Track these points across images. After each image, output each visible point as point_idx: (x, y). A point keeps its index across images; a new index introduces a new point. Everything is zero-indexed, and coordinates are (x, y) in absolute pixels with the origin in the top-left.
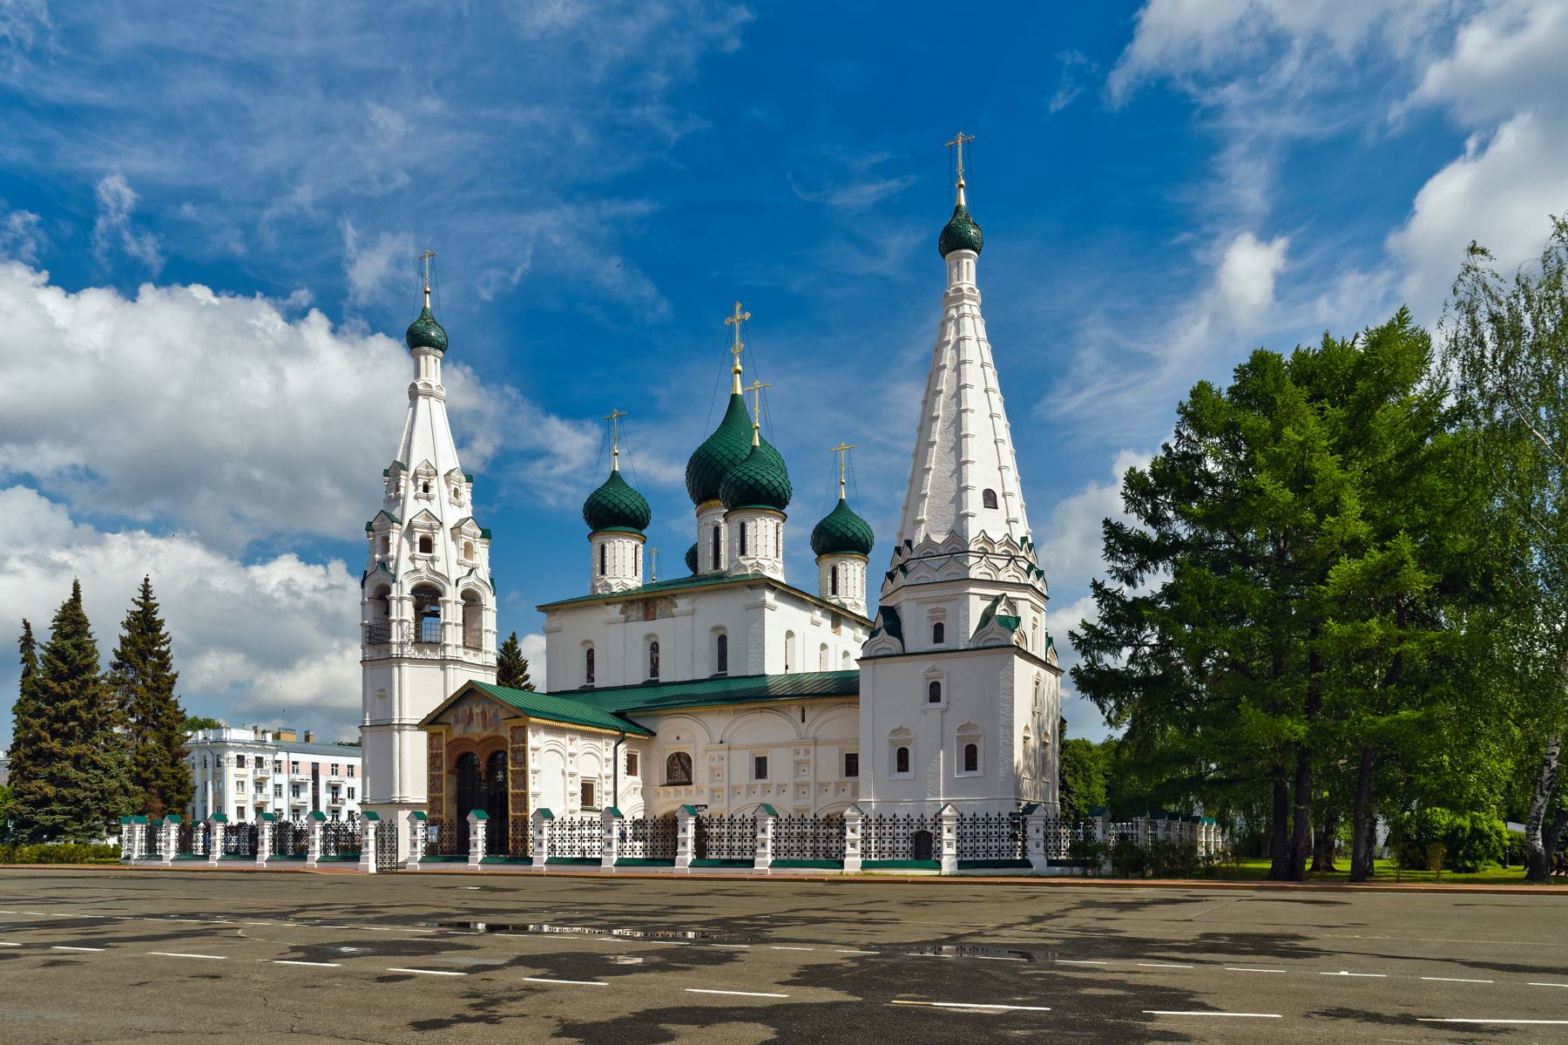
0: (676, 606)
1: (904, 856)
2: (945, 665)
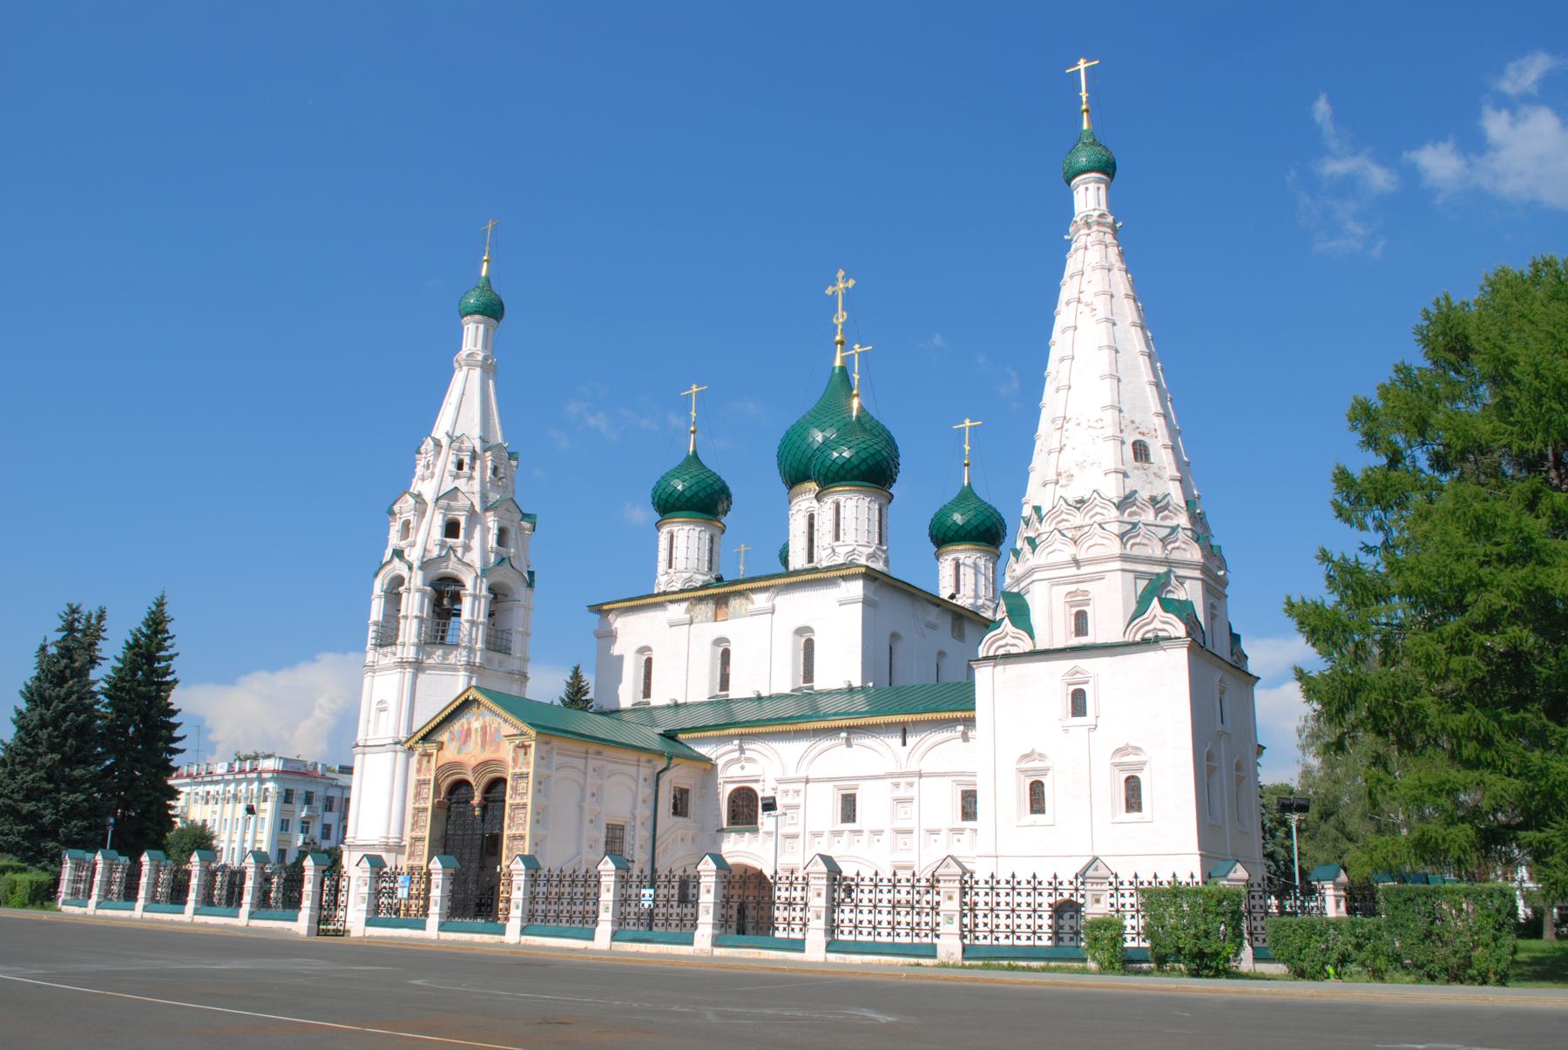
0: (753, 603)
2: (1091, 666)
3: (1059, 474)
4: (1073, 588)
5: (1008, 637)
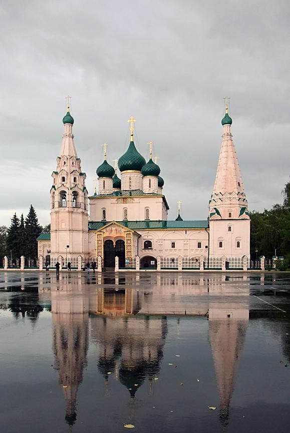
5: (216, 216)
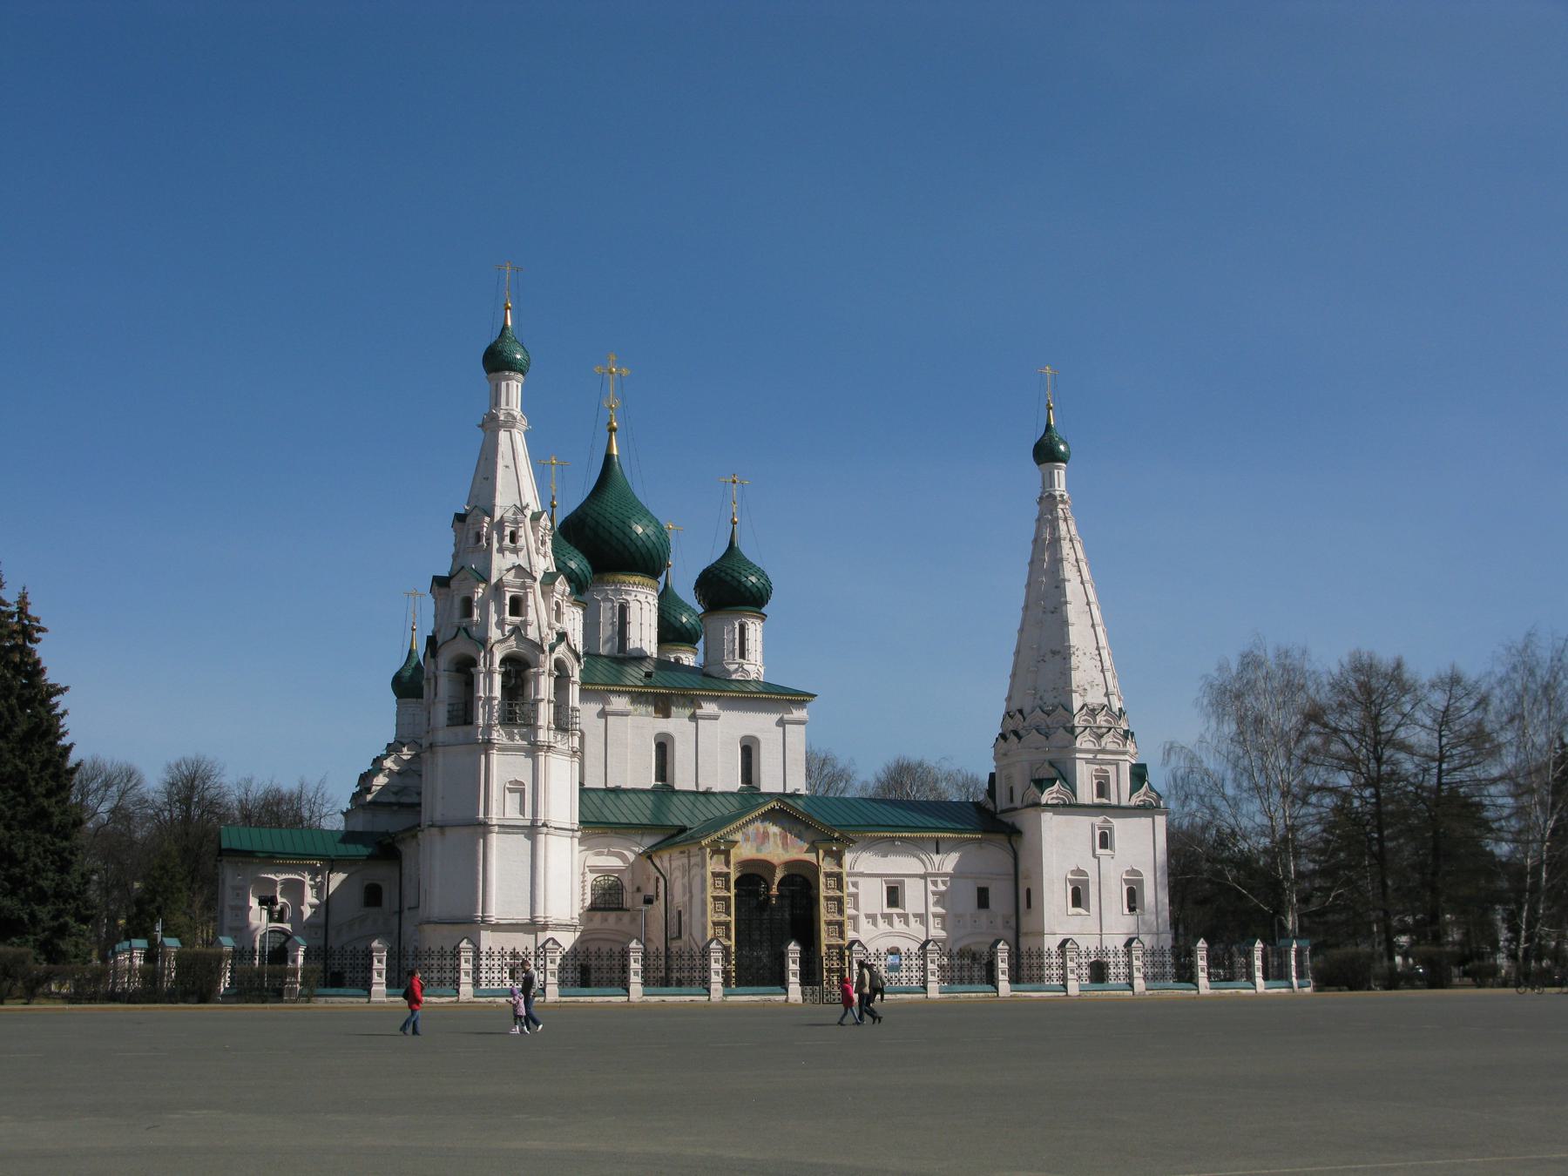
0: (701, 707)
1: (487, 985)
3: (1078, 686)
4: (1097, 767)
